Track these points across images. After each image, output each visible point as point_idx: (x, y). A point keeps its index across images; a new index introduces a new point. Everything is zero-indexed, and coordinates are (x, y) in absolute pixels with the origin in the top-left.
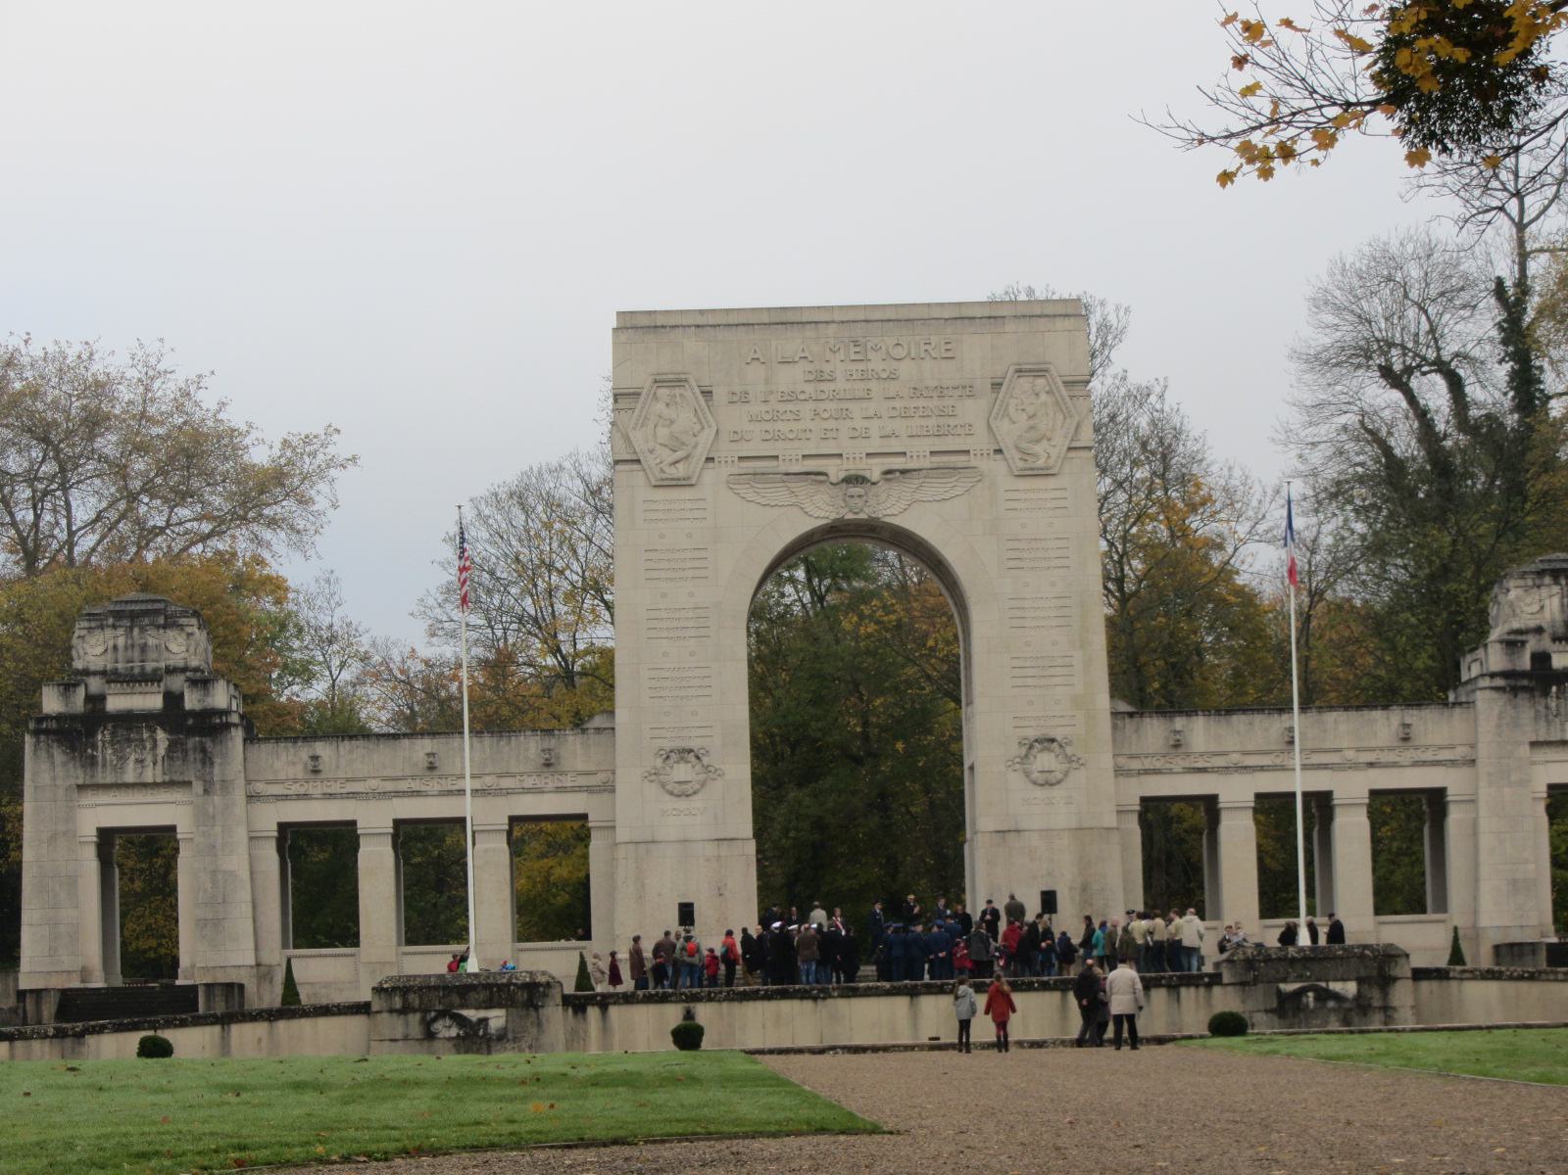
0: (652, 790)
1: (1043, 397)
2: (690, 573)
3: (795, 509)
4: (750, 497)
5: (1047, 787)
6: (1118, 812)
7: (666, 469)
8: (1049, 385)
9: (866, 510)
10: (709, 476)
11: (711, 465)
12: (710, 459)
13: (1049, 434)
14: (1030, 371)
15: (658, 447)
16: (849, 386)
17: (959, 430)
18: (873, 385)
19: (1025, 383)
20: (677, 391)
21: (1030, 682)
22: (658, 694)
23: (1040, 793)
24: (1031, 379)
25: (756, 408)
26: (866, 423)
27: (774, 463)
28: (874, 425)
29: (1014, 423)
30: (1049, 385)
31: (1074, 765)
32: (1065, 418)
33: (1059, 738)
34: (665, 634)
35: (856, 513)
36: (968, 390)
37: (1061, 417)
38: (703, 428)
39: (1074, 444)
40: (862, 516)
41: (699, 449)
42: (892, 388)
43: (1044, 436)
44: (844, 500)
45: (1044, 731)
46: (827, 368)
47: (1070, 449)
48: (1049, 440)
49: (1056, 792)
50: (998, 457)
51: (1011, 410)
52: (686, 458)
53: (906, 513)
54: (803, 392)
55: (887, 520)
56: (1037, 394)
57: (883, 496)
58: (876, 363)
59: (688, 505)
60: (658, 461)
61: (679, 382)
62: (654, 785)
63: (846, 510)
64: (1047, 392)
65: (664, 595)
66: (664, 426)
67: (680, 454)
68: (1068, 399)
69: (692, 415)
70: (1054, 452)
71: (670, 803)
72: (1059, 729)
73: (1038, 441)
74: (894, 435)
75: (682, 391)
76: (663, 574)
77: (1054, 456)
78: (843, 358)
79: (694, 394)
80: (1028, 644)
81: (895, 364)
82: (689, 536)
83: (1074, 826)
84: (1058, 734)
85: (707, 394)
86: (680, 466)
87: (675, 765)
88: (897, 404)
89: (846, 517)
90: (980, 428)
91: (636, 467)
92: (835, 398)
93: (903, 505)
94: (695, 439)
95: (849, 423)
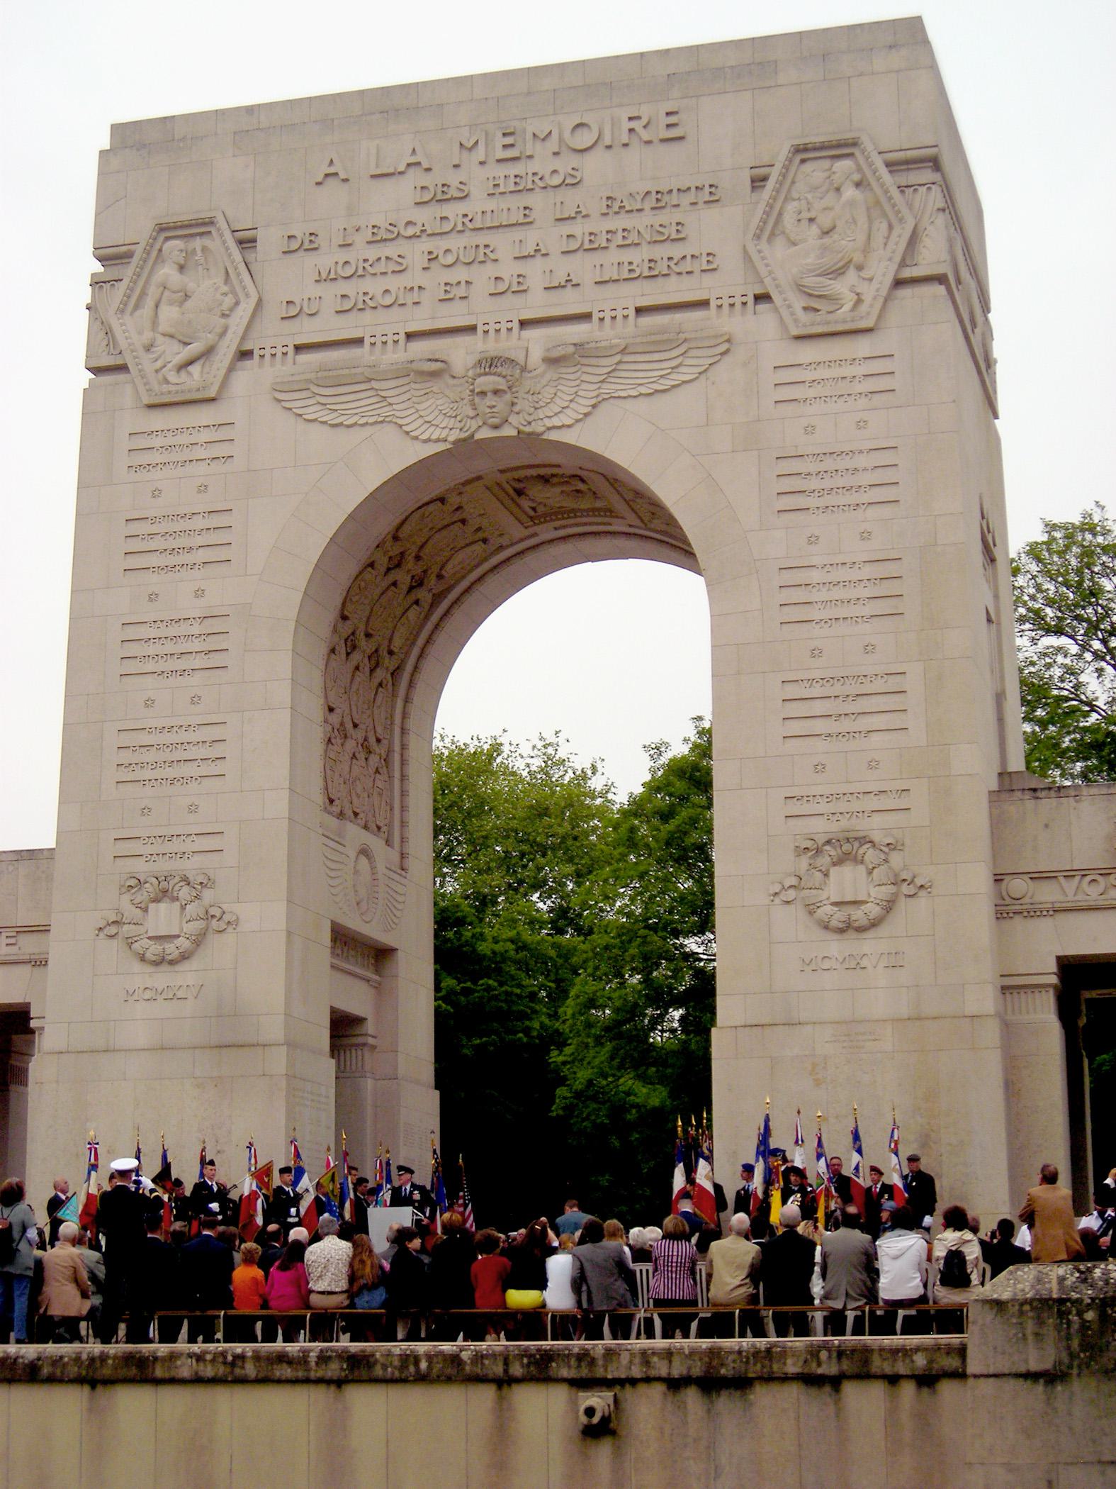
0: (110, 951)
1: (850, 192)
2: (202, 556)
3: (389, 429)
4: (311, 413)
5: (851, 934)
6: (1004, 989)
7: (173, 377)
8: (859, 169)
9: (513, 419)
10: (246, 376)
11: (248, 363)
12: (245, 355)
13: (858, 258)
14: (823, 147)
15: (160, 339)
16: (491, 204)
17: (687, 265)
18: (537, 200)
19: (815, 172)
20: (198, 243)
21: (820, 726)
22: (131, 777)
23: (836, 947)
24: (826, 164)
25: (326, 260)
26: (520, 268)
27: (354, 352)
28: (535, 272)
29: (794, 244)
30: (859, 169)
31: (905, 889)
32: (891, 227)
33: (877, 837)
34: (150, 666)
35: (496, 427)
36: (712, 196)
37: (884, 226)
38: (237, 303)
39: (907, 273)
40: (508, 431)
41: (230, 335)
42: (572, 199)
43: (850, 261)
45: (844, 823)
46: (453, 179)
47: (899, 283)
48: (860, 268)
49: (870, 945)
50: (762, 307)
51: (789, 220)
52: (208, 352)
53: (589, 420)
54: (409, 223)
55: (554, 436)
56: (838, 190)
57: (548, 393)
58: (542, 164)
59: (205, 436)
60: (159, 364)
61: (201, 227)
62: (114, 942)
63: (474, 424)
64: (858, 185)
65: (153, 597)
66: (171, 303)
67: (196, 348)
68: (895, 192)
69: (220, 280)
70: (869, 292)
71: (143, 977)
72: (876, 817)
73: (838, 272)
74: (570, 283)
75: (206, 241)
76: (154, 560)
77: (867, 298)
78: (482, 159)
79: (224, 242)
80: (816, 653)
81: (575, 160)
82: (203, 489)
83: (904, 1012)
84: (876, 827)
85: (247, 243)
86: (195, 369)
87: (152, 906)
88: (579, 228)
89: (478, 436)
90: (729, 259)
91: (121, 377)
92: (468, 225)
93: (582, 406)
94: (223, 321)
95: (490, 270)
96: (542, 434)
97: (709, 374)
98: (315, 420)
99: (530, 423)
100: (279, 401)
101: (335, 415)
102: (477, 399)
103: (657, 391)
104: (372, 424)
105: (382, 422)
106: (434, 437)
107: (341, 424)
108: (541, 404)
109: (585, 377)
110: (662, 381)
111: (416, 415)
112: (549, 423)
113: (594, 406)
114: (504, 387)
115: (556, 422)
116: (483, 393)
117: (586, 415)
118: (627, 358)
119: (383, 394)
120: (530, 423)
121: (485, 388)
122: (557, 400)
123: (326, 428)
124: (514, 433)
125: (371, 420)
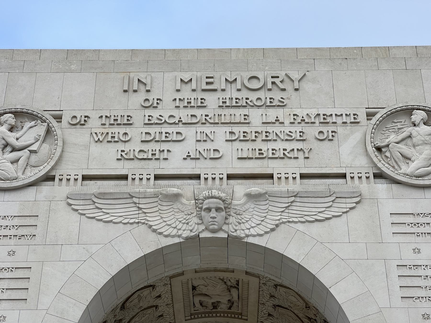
35: (214, 231)
44: (201, 218)
55: (251, 240)
89: (201, 236)
96: (243, 238)
97: (348, 214)
98: (93, 218)
99: (236, 231)
100: (70, 205)
101: (108, 216)
102: (203, 213)
103: (317, 220)
104: (132, 224)
105: (138, 223)
106: (173, 233)
107: (111, 221)
108: (243, 221)
109: (270, 208)
110: (319, 214)
111: (161, 221)
112: (247, 232)
113: (277, 226)
114: (223, 207)
115: (252, 231)
116: (209, 210)
117: (273, 230)
118: (298, 199)
119: (141, 206)
120: (236, 231)
121: (212, 206)
122: (250, 222)
123: (101, 224)
124: (226, 236)
125: (132, 221)
